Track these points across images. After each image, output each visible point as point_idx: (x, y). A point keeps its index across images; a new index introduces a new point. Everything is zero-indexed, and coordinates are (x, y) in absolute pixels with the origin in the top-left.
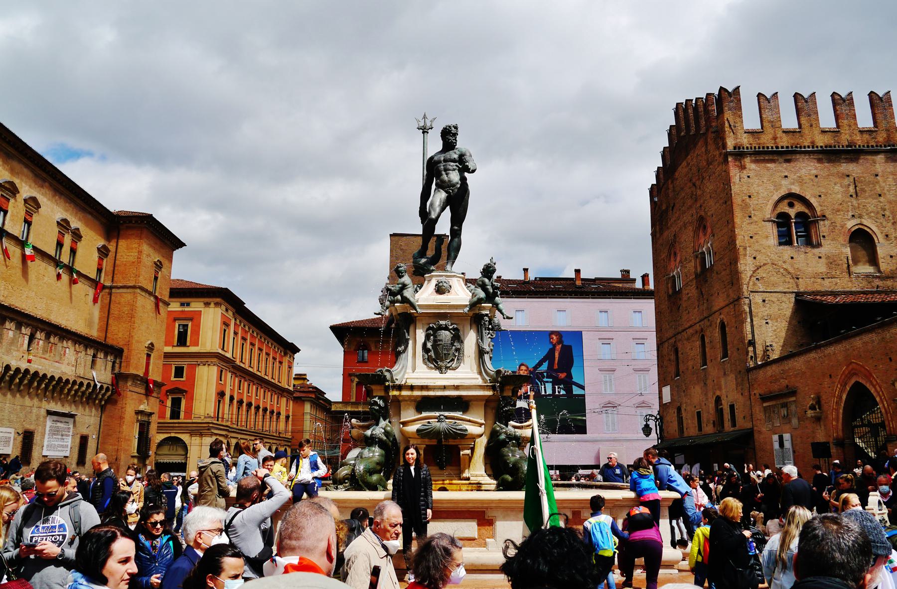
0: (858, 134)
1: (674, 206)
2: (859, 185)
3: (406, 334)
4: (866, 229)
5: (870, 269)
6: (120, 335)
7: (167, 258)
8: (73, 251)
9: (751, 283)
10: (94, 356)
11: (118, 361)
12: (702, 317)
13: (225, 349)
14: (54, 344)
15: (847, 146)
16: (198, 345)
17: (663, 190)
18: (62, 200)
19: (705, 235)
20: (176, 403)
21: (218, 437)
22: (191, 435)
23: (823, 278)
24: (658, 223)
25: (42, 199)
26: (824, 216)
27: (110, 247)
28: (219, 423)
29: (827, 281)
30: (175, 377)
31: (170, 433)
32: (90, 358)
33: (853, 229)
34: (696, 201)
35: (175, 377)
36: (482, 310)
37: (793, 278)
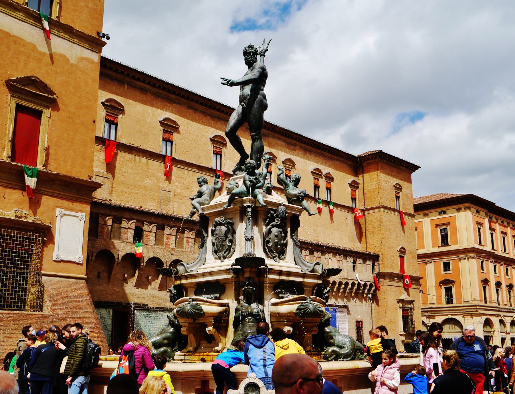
3: (204, 233)
6: (375, 244)
7: (405, 181)
8: (329, 189)
10: (354, 262)
11: (376, 264)
13: (483, 244)
14: (318, 257)
16: (457, 244)
18: (312, 156)
20: (448, 291)
21: (488, 317)
22: (464, 316)
25: (294, 158)
27: (358, 181)
28: (488, 304)
30: (444, 271)
31: (447, 315)
32: (351, 264)
35: (444, 271)
36: (245, 203)
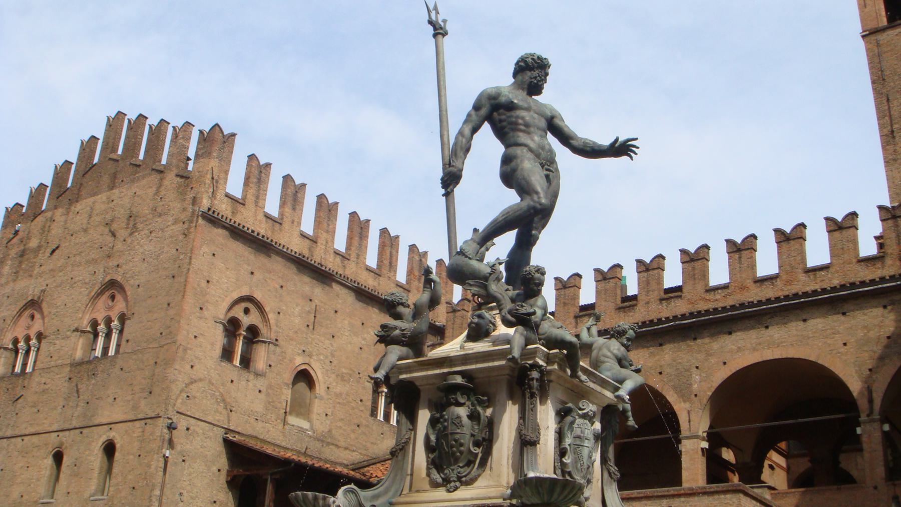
0: (332, 255)
1: (57, 248)
2: (318, 316)
4: (311, 372)
5: (305, 425)
9: (179, 401)
12: (67, 426)
15: (319, 264)
17: (40, 219)
19: (110, 308)
23: (256, 419)
24: (9, 262)
26: (277, 340)
29: (260, 425)
33: (300, 368)
34: (109, 257)
37: (227, 409)
